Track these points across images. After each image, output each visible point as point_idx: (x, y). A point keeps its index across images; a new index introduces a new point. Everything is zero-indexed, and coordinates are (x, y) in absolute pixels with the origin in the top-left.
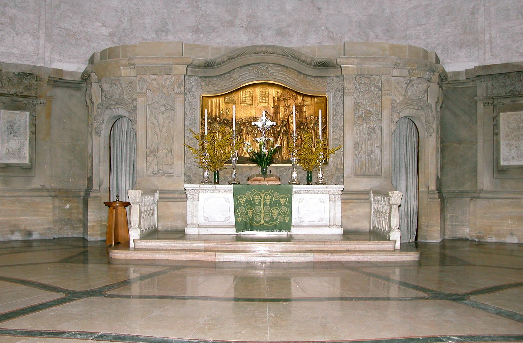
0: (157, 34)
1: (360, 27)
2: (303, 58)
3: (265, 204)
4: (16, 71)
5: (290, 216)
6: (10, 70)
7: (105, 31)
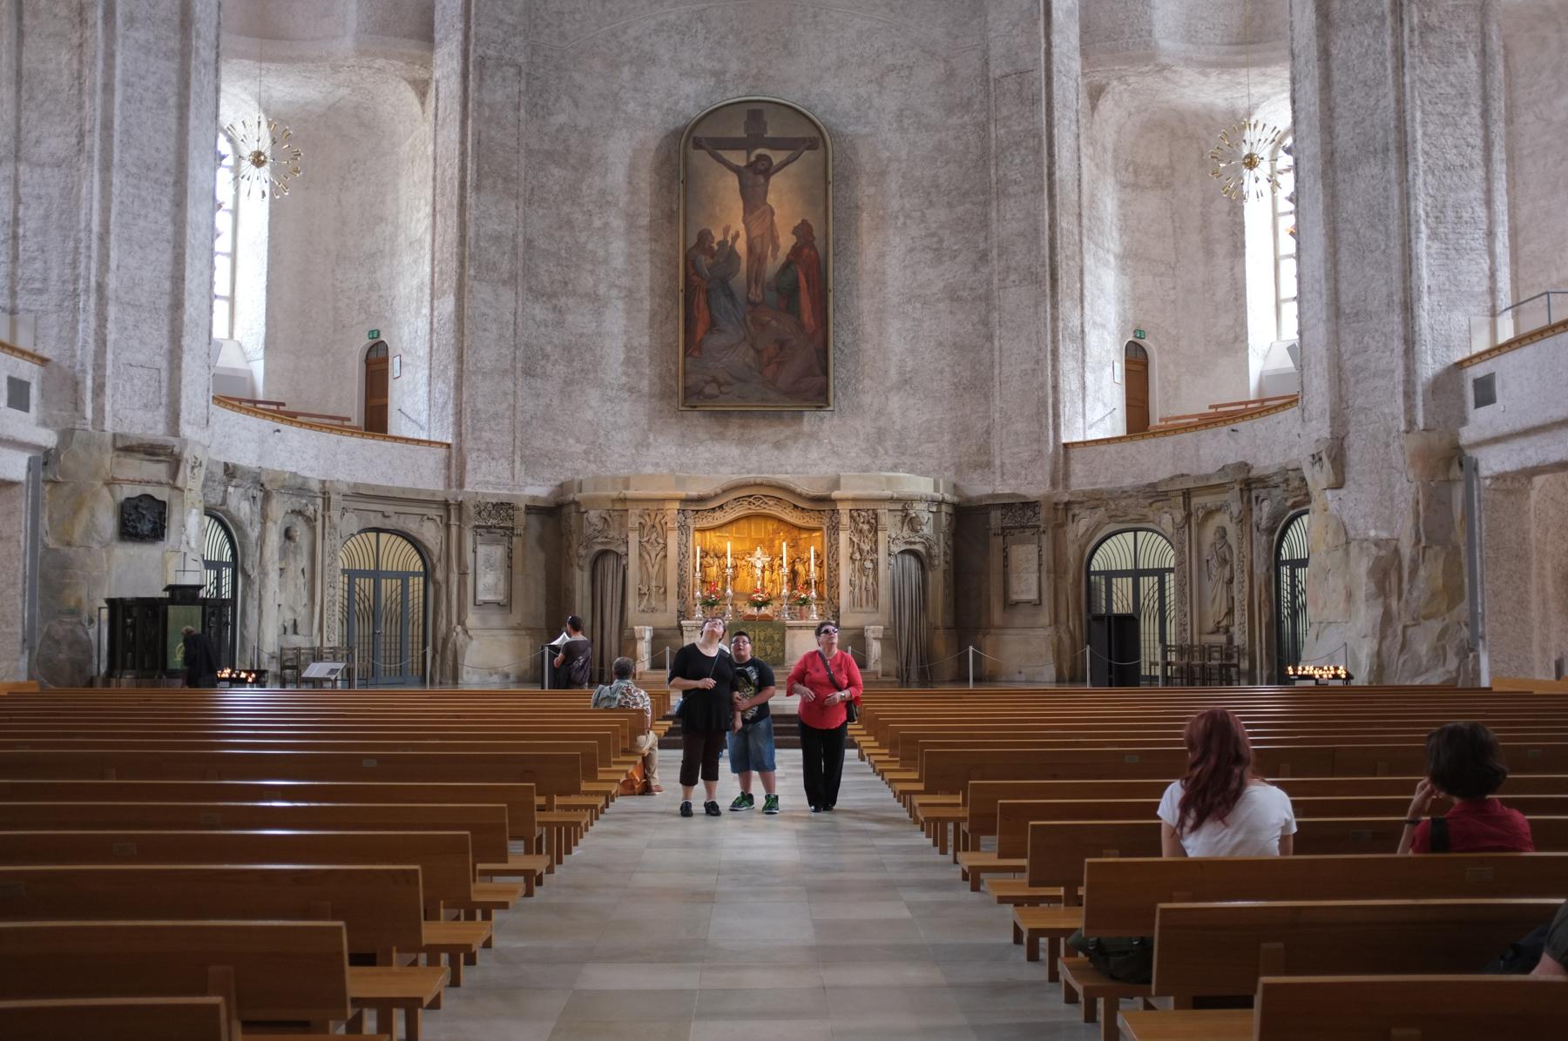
0: (637, 450)
1: (868, 441)
2: (799, 490)
3: (760, 640)
4: (494, 501)
5: (783, 651)
6: (489, 500)
7: (580, 448)
